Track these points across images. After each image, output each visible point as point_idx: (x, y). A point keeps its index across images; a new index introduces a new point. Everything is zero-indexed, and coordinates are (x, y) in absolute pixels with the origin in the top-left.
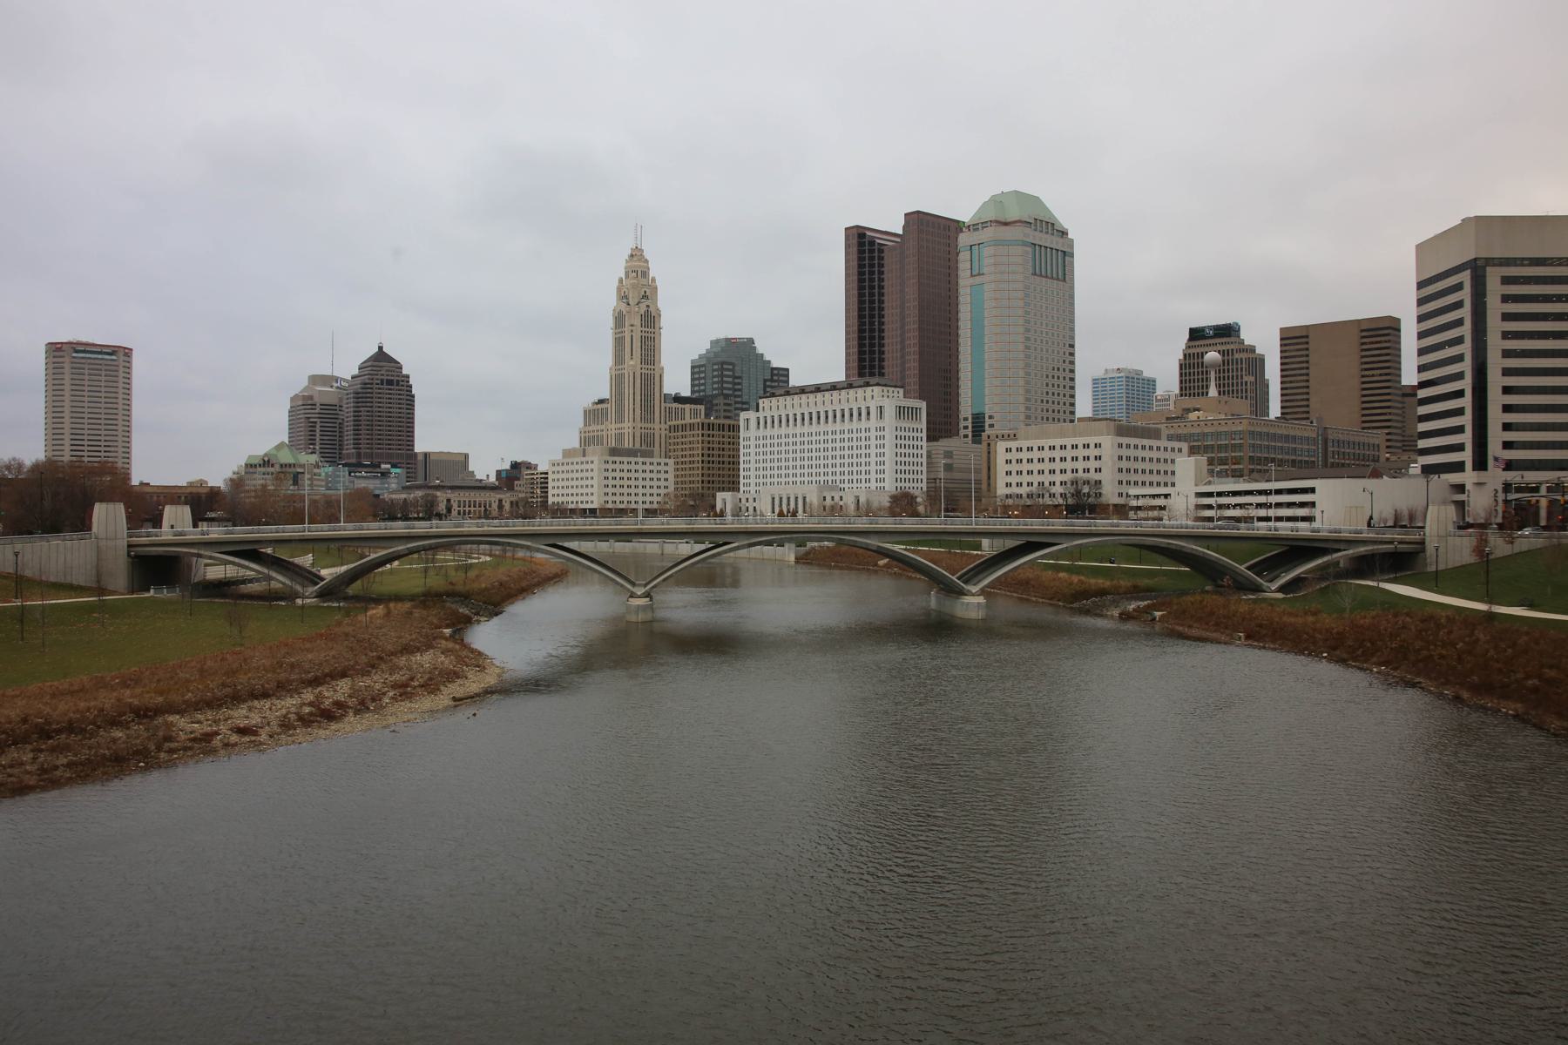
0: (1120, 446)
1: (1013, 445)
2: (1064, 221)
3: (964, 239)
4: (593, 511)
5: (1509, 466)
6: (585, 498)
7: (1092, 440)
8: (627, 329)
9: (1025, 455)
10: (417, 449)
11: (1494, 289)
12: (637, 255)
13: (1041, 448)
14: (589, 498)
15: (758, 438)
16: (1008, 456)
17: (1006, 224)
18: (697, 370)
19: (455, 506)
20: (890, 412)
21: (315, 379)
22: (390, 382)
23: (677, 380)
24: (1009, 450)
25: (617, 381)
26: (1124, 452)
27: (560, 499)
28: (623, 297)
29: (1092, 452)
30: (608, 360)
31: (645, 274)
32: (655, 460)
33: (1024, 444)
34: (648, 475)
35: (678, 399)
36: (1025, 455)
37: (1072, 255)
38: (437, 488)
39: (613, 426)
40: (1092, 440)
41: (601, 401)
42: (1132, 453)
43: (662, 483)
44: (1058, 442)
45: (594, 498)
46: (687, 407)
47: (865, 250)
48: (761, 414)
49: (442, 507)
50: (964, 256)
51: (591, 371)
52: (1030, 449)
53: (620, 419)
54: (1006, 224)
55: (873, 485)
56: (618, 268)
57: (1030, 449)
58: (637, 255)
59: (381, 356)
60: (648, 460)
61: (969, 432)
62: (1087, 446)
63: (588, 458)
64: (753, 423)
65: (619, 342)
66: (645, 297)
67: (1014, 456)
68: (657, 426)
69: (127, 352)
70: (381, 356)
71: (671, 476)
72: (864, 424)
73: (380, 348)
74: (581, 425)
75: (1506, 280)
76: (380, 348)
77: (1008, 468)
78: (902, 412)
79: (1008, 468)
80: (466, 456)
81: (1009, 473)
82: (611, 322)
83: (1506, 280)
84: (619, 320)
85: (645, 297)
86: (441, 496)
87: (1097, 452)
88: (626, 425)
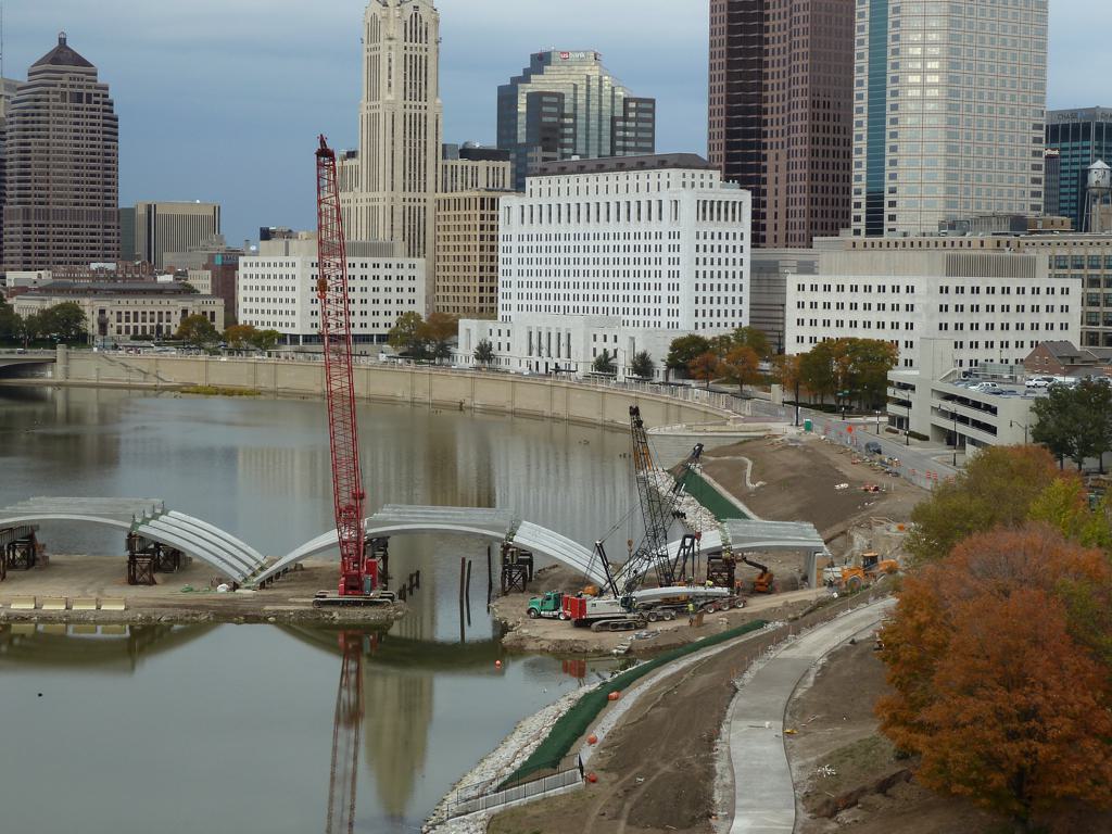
0: (944, 290)
1: (807, 280)
4: (294, 339)
6: (284, 319)
7: (903, 282)
8: (384, 44)
9: (820, 297)
10: (124, 202)
14: (290, 319)
15: (521, 238)
16: (801, 297)
19: (113, 319)
20: (688, 210)
22: (79, 97)
24: (801, 288)
26: (952, 300)
27: (253, 317)
29: (903, 299)
32: (394, 261)
33: (821, 280)
34: (382, 284)
35: (467, 153)
36: (820, 297)
38: (85, 292)
39: (365, 195)
42: (967, 300)
45: (295, 319)
46: (482, 164)
48: (526, 200)
49: (91, 326)
52: (827, 288)
53: (373, 185)
57: (827, 288)
59: (63, 55)
60: (382, 261)
61: (862, 226)
62: (896, 289)
63: (290, 259)
64: (516, 213)
67: (808, 297)
68: (431, 196)
70: (63, 55)
72: (654, 227)
73: (62, 41)
76: (62, 41)
77: (799, 314)
78: (707, 209)
79: (799, 314)
81: (800, 322)
86: (89, 307)
88: (380, 195)
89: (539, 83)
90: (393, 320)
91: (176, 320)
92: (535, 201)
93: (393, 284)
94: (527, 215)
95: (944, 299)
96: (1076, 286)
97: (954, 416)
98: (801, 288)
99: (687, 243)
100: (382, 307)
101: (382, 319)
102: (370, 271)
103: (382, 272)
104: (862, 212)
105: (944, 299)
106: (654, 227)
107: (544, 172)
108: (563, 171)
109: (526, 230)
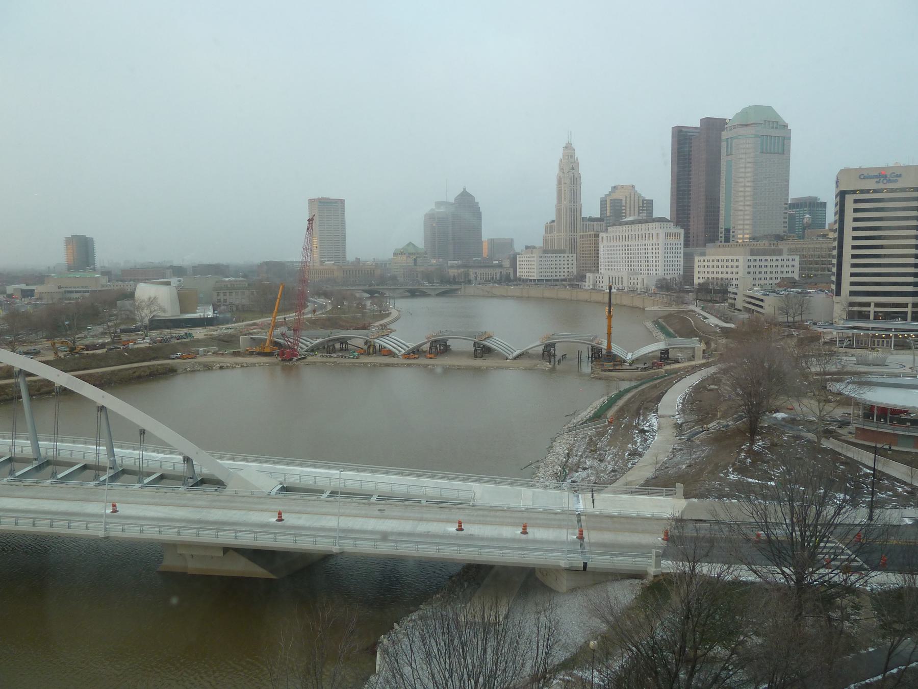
1: (702, 258)
2: (786, 117)
3: (725, 135)
4: (534, 280)
5: (852, 293)
7: (735, 258)
8: (563, 186)
9: (706, 264)
11: (850, 205)
12: (568, 147)
13: (713, 261)
17: (747, 125)
18: (603, 202)
20: (662, 236)
21: (439, 204)
23: (591, 208)
24: (699, 261)
25: (559, 211)
26: (752, 264)
28: (562, 169)
30: (555, 201)
31: (573, 156)
36: (706, 264)
37: (790, 138)
38: (470, 267)
40: (735, 258)
41: (553, 221)
43: (570, 266)
44: (720, 258)
47: (683, 140)
48: (608, 235)
49: (472, 277)
50: (724, 144)
51: (546, 207)
53: (560, 231)
54: (747, 125)
55: (654, 272)
56: (559, 154)
57: (709, 261)
58: (568, 147)
62: (732, 260)
64: (605, 238)
65: (559, 192)
66: (572, 168)
67: (702, 264)
69: (342, 201)
71: (574, 263)
74: (544, 233)
75: (856, 201)
77: (699, 269)
78: (668, 235)
79: (699, 269)
80: (512, 240)
81: (699, 272)
82: (556, 182)
83: (856, 201)
84: (560, 182)
85: (572, 168)
86: (472, 272)
87: (736, 264)
89: (615, 196)
90: (566, 274)
91: (498, 275)
92: (611, 235)
93: (566, 262)
94: (608, 239)
95: (750, 264)
96: (797, 258)
97: (750, 303)
98: (699, 261)
99: (661, 246)
100: (562, 270)
101: (562, 274)
102: (558, 259)
103: (562, 259)
104: (723, 235)
105: (750, 264)
106: (650, 242)
107: (614, 225)
108: (621, 224)
109: (608, 244)
